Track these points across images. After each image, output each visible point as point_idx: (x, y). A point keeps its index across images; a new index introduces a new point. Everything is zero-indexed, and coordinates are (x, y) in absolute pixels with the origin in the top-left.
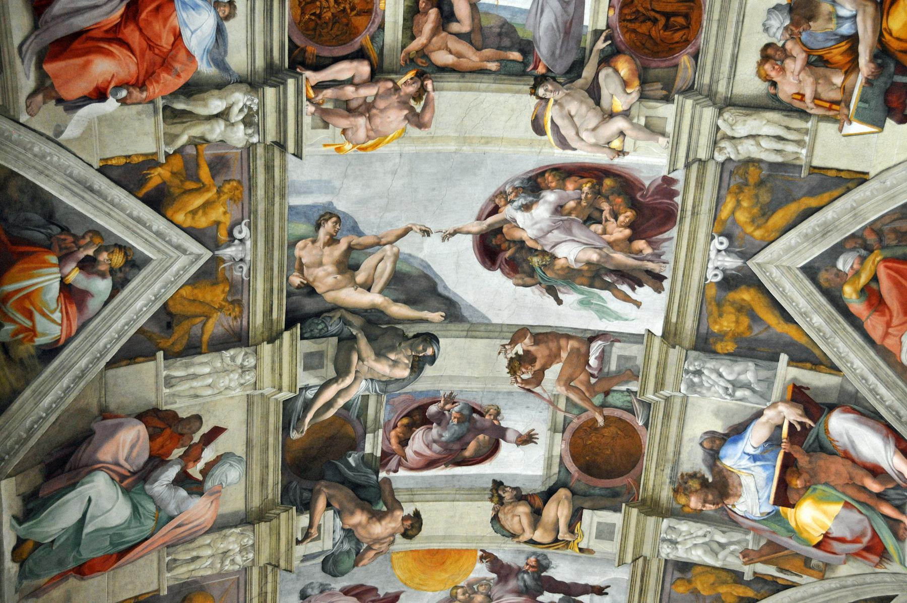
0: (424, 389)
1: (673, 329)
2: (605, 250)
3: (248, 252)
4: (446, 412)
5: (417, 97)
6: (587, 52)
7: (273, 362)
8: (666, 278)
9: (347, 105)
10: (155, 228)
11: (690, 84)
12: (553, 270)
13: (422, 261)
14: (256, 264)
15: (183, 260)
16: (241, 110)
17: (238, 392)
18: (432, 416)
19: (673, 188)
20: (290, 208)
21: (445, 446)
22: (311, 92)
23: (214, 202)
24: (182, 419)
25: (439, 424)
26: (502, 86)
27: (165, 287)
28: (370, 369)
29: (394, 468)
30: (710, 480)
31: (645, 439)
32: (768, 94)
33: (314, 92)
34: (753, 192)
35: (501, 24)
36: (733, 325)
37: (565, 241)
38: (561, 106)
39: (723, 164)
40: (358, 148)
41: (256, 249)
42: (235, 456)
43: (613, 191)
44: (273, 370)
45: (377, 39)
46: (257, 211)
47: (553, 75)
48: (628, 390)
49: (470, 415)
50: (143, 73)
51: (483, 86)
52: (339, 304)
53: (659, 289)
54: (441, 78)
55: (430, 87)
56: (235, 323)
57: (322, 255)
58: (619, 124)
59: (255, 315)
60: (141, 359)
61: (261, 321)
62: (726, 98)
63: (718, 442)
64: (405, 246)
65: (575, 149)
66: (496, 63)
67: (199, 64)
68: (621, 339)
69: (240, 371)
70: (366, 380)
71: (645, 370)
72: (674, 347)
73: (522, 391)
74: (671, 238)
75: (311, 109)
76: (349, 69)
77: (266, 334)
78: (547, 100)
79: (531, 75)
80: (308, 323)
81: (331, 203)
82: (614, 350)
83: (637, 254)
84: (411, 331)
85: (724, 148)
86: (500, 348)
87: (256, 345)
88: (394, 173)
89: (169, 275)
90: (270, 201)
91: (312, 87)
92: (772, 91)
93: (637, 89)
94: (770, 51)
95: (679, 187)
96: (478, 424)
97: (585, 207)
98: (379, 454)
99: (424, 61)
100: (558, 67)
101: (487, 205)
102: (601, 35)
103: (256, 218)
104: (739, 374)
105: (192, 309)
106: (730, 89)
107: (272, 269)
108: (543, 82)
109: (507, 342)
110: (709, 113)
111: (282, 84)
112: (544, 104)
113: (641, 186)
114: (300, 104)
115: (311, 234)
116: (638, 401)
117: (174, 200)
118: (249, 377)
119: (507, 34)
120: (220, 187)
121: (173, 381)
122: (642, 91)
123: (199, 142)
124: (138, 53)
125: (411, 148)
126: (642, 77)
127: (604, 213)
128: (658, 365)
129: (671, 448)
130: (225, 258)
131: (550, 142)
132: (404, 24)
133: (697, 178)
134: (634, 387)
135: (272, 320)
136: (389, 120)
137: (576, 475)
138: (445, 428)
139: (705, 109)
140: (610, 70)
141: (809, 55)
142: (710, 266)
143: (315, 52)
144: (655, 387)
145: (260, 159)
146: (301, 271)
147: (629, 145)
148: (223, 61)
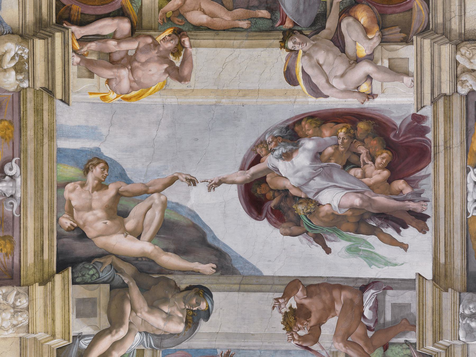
0: (202, 347)
1: (442, 271)
2: (366, 194)
3: (19, 189)
5: (176, 52)
6: (328, 5)
7: (45, 306)
8: (429, 217)
9: (110, 57)
13: (190, 210)
14: (26, 202)
16: (13, 58)
17: (10, 333)
19: (424, 125)
20: (59, 150)
22: (77, 46)
26: (254, 42)
33: (80, 45)
37: (327, 188)
38: (310, 56)
39: (467, 96)
40: (121, 98)
41: (26, 187)
44: (45, 313)
46: (26, 151)
47: (300, 29)
51: (236, 42)
52: (110, 250)
53: (423, 230)
55: (187, 44)
56: (6, 260)
57: (91, 200)
58: (366, 68)
59: (27, 253)
61: (33, 262)
62: (460, 34)
65: (327, 97)
66: (247, 22)
69: (12, 311)
70: (140, 333)
71: (421, 318)
72: (447, 291)
73: (299, 348)
74: (429, 175)
75: (77, 59)
76: (112, 26)
77: (38, 275)
81: (98, 149)
82: (388, 298)
83: (397, 195)
84: (184, 282)
85: (466, 81)
86: (272, 302)
88: (159, 123)
90: (39, 142)
91: (78, 40)
93: (377, 34)
95: (429, 123)
97: (343, 152)
100: (303, 21)
101: (249, 155)
103: (26, 157)
106: (463, 25)
107: (42, 209)
110: (446, 50)
111: (50, 36)
112: (294, 56)
113: (394, 127)
114: (66, 55)
118: (22, 319)
122: (383, 35)
126: (381, 25)
127: (362, 156)
128: (433, 312)
133: (445, 113)
139: (442, 47)
140: (351, 20)
142: (470, 199)
143: (80, 10)
144: (433, 335)
145: (30, 103)
146: (71, 213)
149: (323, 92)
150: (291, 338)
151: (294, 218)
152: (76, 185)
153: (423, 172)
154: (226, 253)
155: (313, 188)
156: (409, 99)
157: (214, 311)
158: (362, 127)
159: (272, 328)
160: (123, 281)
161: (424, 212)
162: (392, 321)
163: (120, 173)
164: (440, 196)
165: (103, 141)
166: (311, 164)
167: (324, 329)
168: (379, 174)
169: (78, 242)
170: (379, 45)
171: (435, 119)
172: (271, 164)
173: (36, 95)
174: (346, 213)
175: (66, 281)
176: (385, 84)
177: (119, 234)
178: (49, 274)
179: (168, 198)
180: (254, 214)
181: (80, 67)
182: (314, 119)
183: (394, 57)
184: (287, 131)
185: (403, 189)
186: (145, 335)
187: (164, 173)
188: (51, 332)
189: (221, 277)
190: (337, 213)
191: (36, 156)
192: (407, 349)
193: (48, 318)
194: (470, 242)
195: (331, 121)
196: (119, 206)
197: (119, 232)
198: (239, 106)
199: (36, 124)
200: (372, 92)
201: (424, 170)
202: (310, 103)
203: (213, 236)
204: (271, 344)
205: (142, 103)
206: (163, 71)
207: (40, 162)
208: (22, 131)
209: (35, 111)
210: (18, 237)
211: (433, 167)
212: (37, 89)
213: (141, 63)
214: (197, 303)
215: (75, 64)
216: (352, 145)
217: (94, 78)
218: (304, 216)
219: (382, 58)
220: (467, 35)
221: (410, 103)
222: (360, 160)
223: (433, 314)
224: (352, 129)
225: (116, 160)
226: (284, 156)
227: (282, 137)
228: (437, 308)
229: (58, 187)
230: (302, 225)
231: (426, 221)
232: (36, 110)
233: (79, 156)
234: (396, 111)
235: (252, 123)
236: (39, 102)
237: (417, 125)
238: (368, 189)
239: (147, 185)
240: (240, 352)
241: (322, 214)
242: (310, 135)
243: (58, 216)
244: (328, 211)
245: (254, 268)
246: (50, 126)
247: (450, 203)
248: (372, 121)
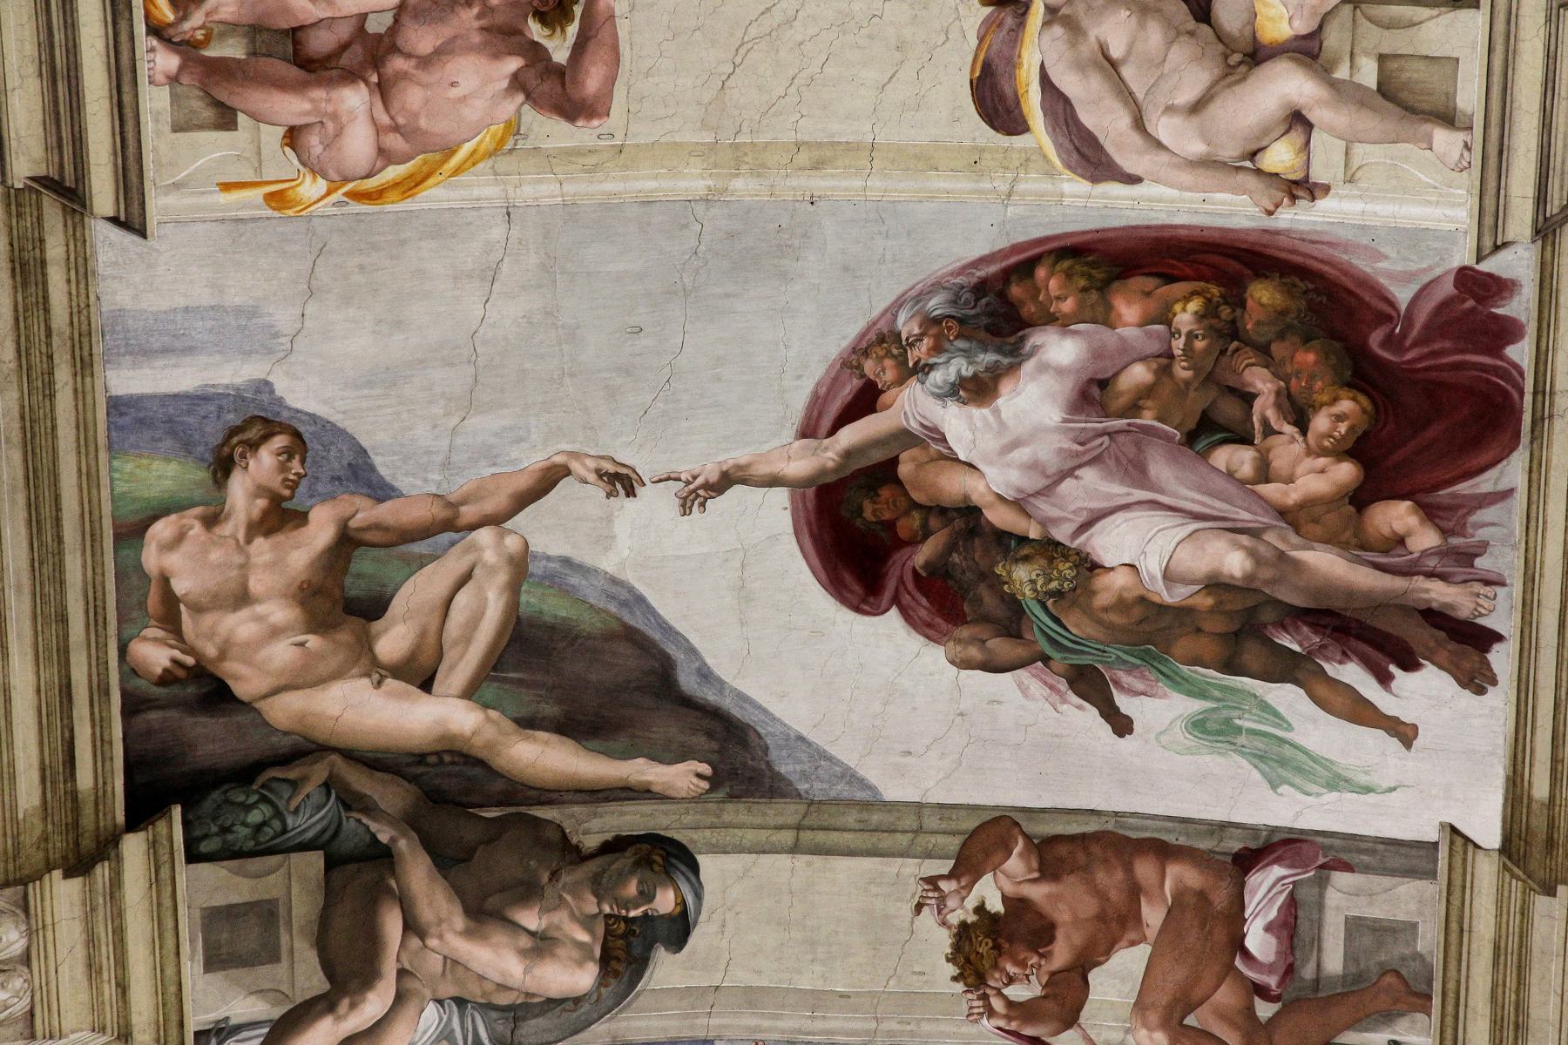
1: (1539, 823)
2: (1270, 537)
7: (91, 941)
8: (1498, 638)
9: (296, 43)
12: (1088, 611)
13: (614, 581)
19: (1499, 311)
20: (117, 405)
28: (452, 963)
38: (1074, 28)
40: (346, 194)
43: (1284, 326)
52: (321, 735)
53: (1477, 680)
57: (244, 567)
65: (1134, 180)
68: (1355, 859)
70: (440, 1002)
71: (1452, 973)
72: (1551, 892)
74: (1507, 494)
75: (168, 61)
77: (58, 844)
80: (208, 805)
81: (265, 386)
82: (1332, 897)
83: (1386, 552)
86: (915, 890)
87: (24, 882)
88: (491, 275)
95: (1520, 307)
97: (1187, 383)
101: (834, 383)
107: (63, 619)
109: (945, 867)
112: (1010, 21)
115: (198, 494)
125: (544, 189)
127: (1258, 404)
136: (454, 93)
149: (1119, 159)
150: (981, 1010)
151: (1000, 612)
152: (185, 521)
153: (1487, 480)
154: (748, 725)
155: (1072, 507)
156: (1448, 212)
157: (703, 917)
158: (1265, 300)
159: (915, 973)
160: (374, 836)
161: (1480, 621)
162: (1344, 977)
163: (349, 464)
164: (1547, 571)
165: (282, 355)
166: (1065, 421)
167: (1101, 984)
168: (1323, 471)
169: (202, 719)
171: (1546, 292)
172: (918, 417)
173: (13, 207)
174: (1190, 602)
176: (1359, 150)
177: (353, 677)
178: (98, 837)
179: (531, 542)
180: (852, 592)
181: (179, 89)
182: (1083, 260)
183: (1399, 52)
184: (977, 300)
185: (1409, 533)
186: (455, 1008)
187: (514, 455)
188: (116, 1026)
189: (730, 807)
190: (1156, 599)
191: (29, 435)
193: (102, 982)
195: (1146, 271)
196: (348, 581)
197: (354, 671)
198: (797, 204)
199: (21, 319)
200: (1307, 176)
201: (1491, 474)
202: (1067, 201)
203: (699, 670)
204: (908, 1028)
205: (425, 206)
206: (505, 83)
207: (44, 455)
209: (13, 270)
211: (1527, 465)
212: (21, 186)
213: (418, 57)
214: (641, 893)
215: (160, 78)
216: (1224, 360)
217: (236, 129)
218: (1035, 602)
219: (1352, 55)
221: (1452, 227)
222: (1249, 415)
223: (1496, 963)
224: (1226, 303)
225: (332, 419)
226: (965, 389)
227: (961, 321)
228: (1510, 944)
229: (118, 538)
230: (1028, 636)
231: (1487, 651)
232: (17, 266)
233: (191, 420)
234: (1398, 252)
235: (846, 269)
236: (30, 235)
237: (1472, 310)
238: (1275, 523)
239: (452, 498)
241: (1102, 600)
242: (1065, 316)
243: (125, 635)
244: (1123, 589)
245: (850, 777)
246: (75, 320)
248: (1302, 280)
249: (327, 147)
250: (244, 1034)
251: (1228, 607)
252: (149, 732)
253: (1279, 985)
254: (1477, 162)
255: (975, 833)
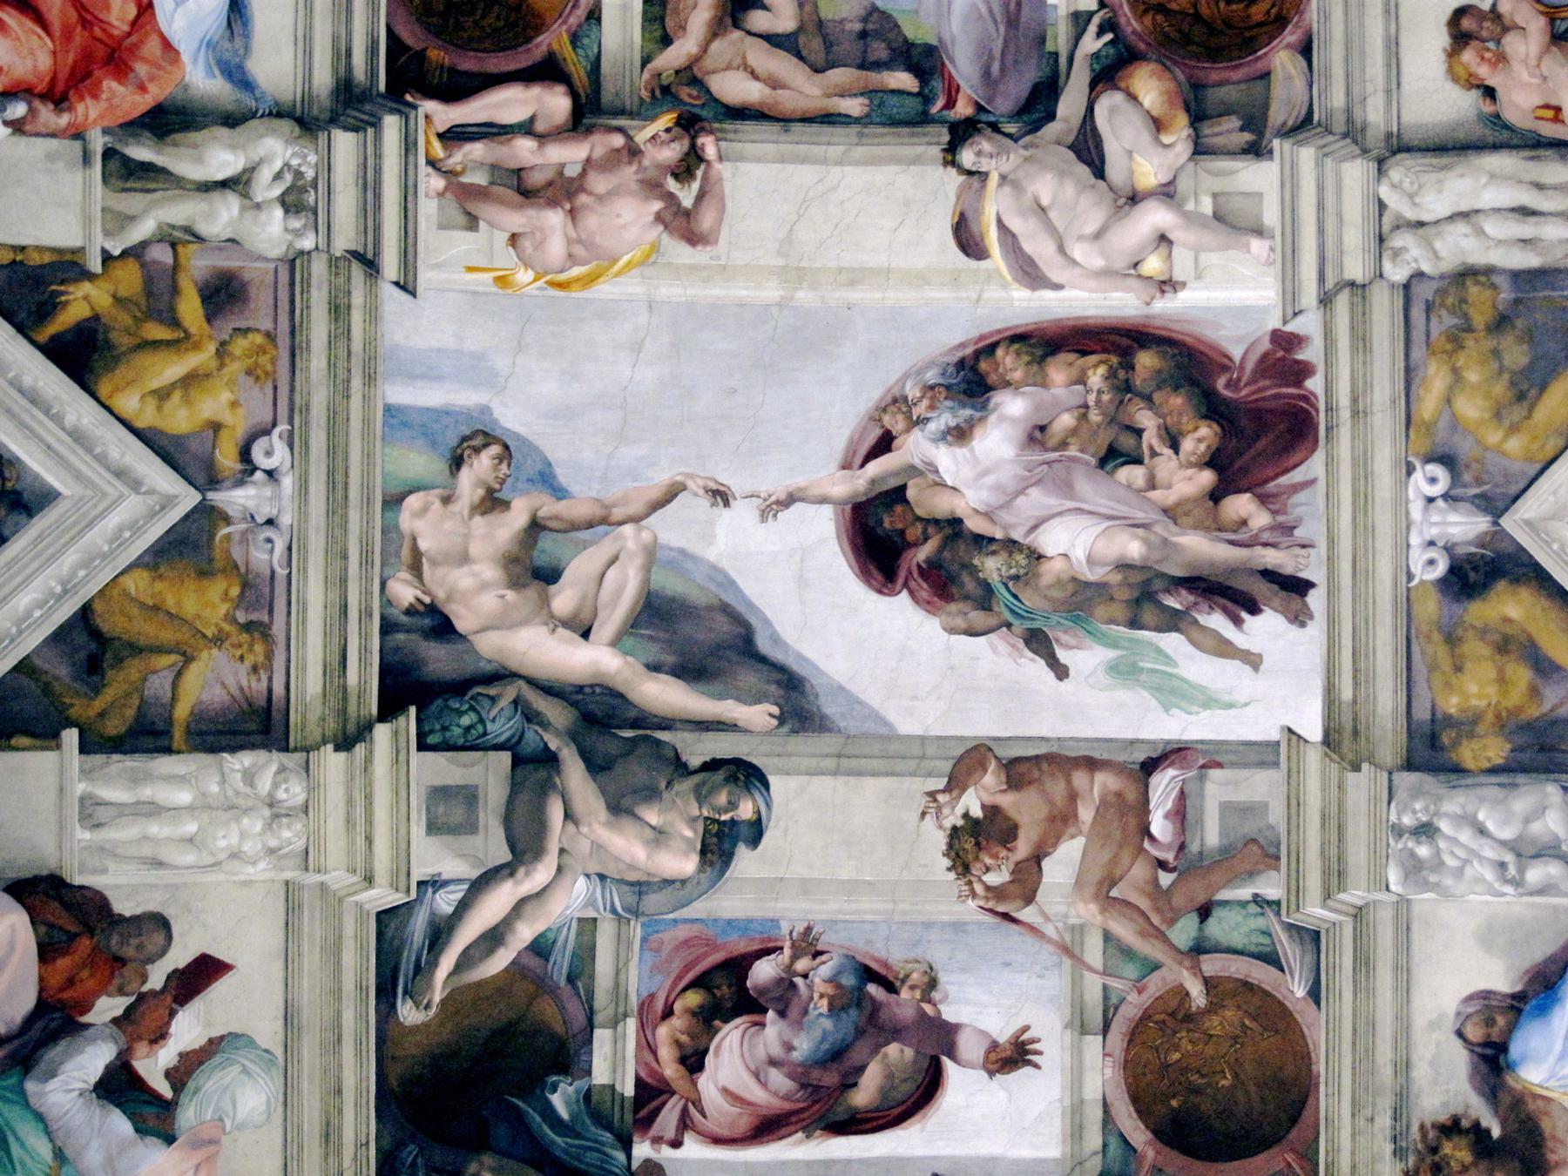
2: (1158, 529)
4: (799, 981)
6: (1063, 61)
7: (350, 802)
9: (519, 179)
10: (70, 420)
11: (1304, 112)
12: (1037, 589)
13: (714, 567)
14: (306, 538)
15: (131, 507)
16: (278, 176)
17: (260, 870)
18: (763, 991)
19: (1300, 357)
20: (389, 410)
21: (802, 1075)
22: (438, 150)
23: (208, 376)
24: (121, 919)
25: (782, 1014)
26: (877, 150)
27: (86, 563)
28: (597, 847)
29: (670, 1133)
30: (1496, 1132)
31: (1318, 1039)
32: (1481, 116)
33: (445, 147)
34: (1490, 343)
35: (863, 12)
36: (1492, 690)
37: (1060, 514)
38: (1017, 187)
39: (1407, 287)
42: (257, 1047)
44: (349, 822)
45: (586, 41)
47: (992, 119)
48: (1257, 899)
49: (860, 989)
50: (63, 75)
51: (835, 151)
52: (514, 665)
53: (1299, 618)
54: (735, 132)
56: (254, 684)
57: (467, 536)
58: (1155, 216)
59: (304, 669)
60: (25, 741)
62: (1389, 135)
63: (1501, 1021)
64: (670, 528)
65: (1058, 287)
66: (861, 100)
67: (189, 68)
69: (267, 812)
70: (588, 876)
73: (988, 919)
74: (1311, 483)
75: (438, 183)
76: (525, 102)
77: (332, 725)
78: (983, 176)
79: (942, 122)
83: (1235, 531)
84: (697, 750)
85: (1404, 249)
87: (307, 750)
88: (637, 348)
89: (98, 536)
91: (441, 136)
92: (1488, 108)
94: (1467, 23)
95: (1311, 353)
96: (884, 1016)
98: (629, 1090)
99: (695, 93)
100: (999, 100)
102: (1089, 21)
103: (306, 423)
104: (1527, 821)
105: (146, 630)
107: (345, 557)
108: (971, 136)
109: (941, 783)
110: (1356, 172)
111: (372, 125)
113: (1226, 361)
116: (1290, 927)
117: (117, 360)
118: (291, 834)
119: (878, 35)
120: (223, 344)
121: (102, 814)
123: (180, 238)
124: (56, 27)
127: (1145, 435)
129: (1385, 1054)
130: (231, 513)
131: (1001, 275)
132: (645, 13)
134: (1271, 887)
135: (345, 688)
137: (1151, 1154)
138: (799, 1025)
141: (1552, 20)
142: (1415, 540)
145: (319, 288)
147: (1182, 264)
148: (240, 67)
157: (772, 823)
169: (432, 644)
170: (1190, 160)
174: (1105, 579)
175: (402, 739)
176: (1204, 256)
181: (443, 201)
185: (1250, 516)
192: (1256, 915)
194: (1415, 649)
196: (535, 553)
206: (651, 218)
208: (298, 358)
210: (283, 627)
214: (730, 802)
220: (1406, 138)
221: (1265, 303)
230: (996, 609)
233: (436, 426)
237: (1283, 359)
239: (607, 502)
240: (840, 926)
247: (1366, 550)
249: (536, 248)
250: (452, 888)
251: (1132, 580)
252: (397, 649)
253: (1176, 858)
254: (1279, 260)
255: (961, 758)
